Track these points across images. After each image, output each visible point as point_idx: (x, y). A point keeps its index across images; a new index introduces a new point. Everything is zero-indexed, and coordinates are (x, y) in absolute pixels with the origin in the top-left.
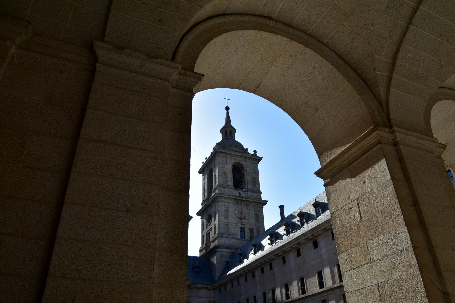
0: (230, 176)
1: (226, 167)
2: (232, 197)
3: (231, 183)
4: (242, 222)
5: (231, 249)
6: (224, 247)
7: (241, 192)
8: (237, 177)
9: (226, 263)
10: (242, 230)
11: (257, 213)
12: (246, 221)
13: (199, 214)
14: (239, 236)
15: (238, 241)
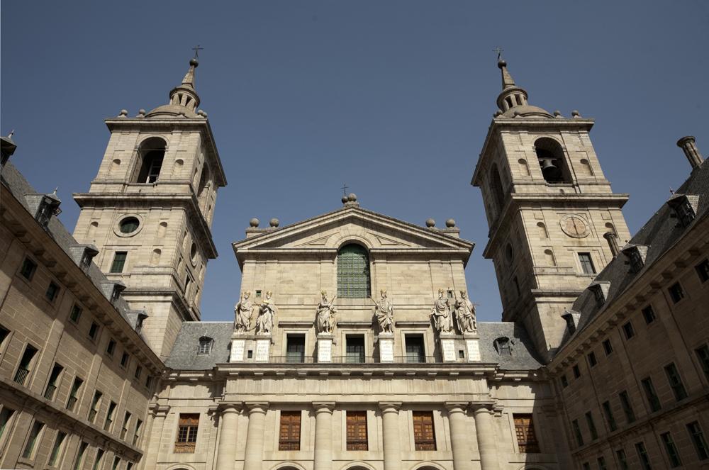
0: (534, 161)
1: (522, 148)
2: (548, 198)
3: (538, 175)
4: (579, 242)
5: (567, 295)
6: (553, 295)
7: (563, 188)
8: (549, 164)
9: (564, 323)
10: (586, 256)
11: (610, 221)
12: (589, 239)
13: (488, 254)
14: (580, 270)
15: (579, 280)
